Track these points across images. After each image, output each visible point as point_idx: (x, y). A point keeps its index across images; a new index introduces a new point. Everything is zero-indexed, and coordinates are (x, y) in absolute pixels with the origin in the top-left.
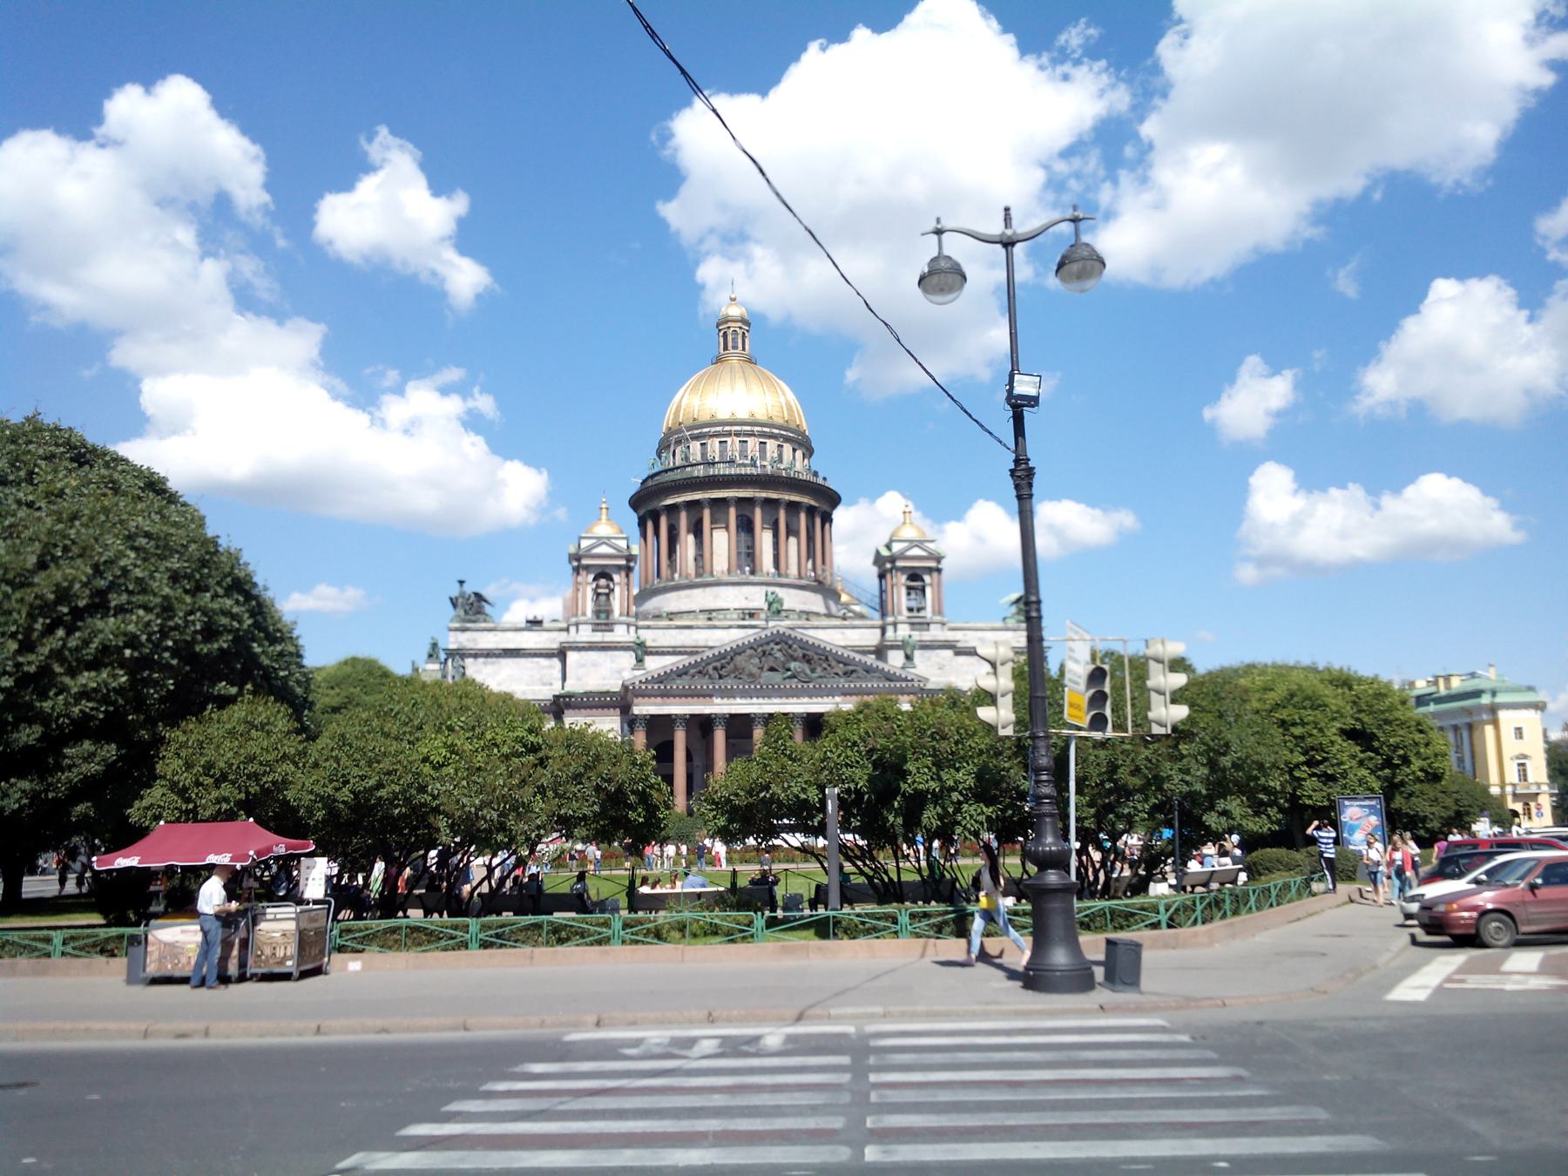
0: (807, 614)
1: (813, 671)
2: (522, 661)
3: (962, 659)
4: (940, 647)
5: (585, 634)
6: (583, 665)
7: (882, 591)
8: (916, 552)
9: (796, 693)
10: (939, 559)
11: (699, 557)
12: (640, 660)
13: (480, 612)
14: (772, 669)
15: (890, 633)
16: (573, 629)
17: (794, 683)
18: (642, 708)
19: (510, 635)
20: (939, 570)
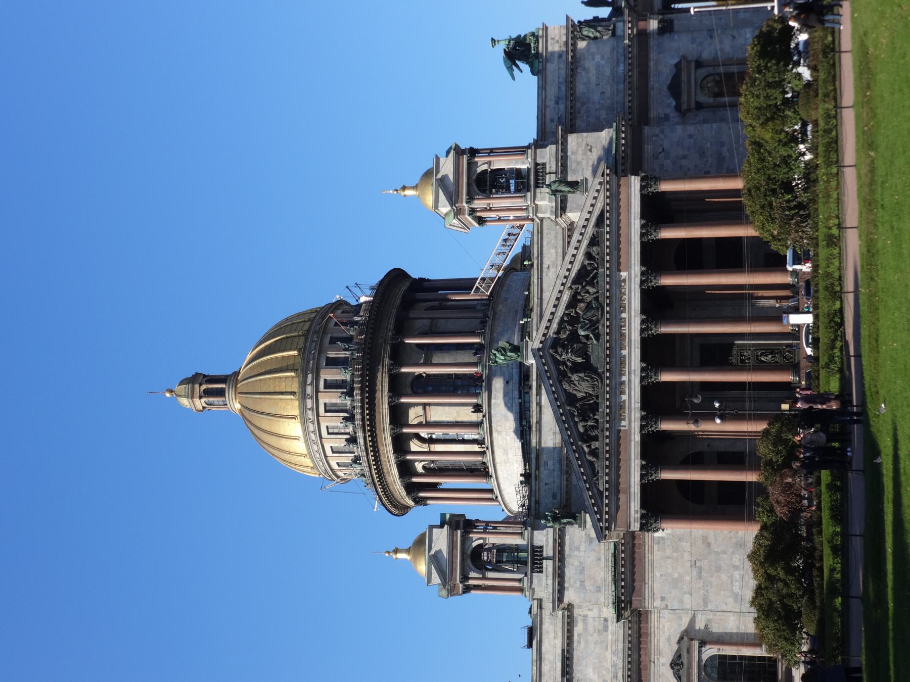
2: (576, 654)
3: (579, 123)
4: (564, 150)
5: (543, 584)
6: (582, 582)
7: (500, 219)
9: (617, 327)
10: (459, 152)
14: (587, 357)
16: (539, 594)
17: (603, 330)
19: (546, 668)
20: (473, 152)
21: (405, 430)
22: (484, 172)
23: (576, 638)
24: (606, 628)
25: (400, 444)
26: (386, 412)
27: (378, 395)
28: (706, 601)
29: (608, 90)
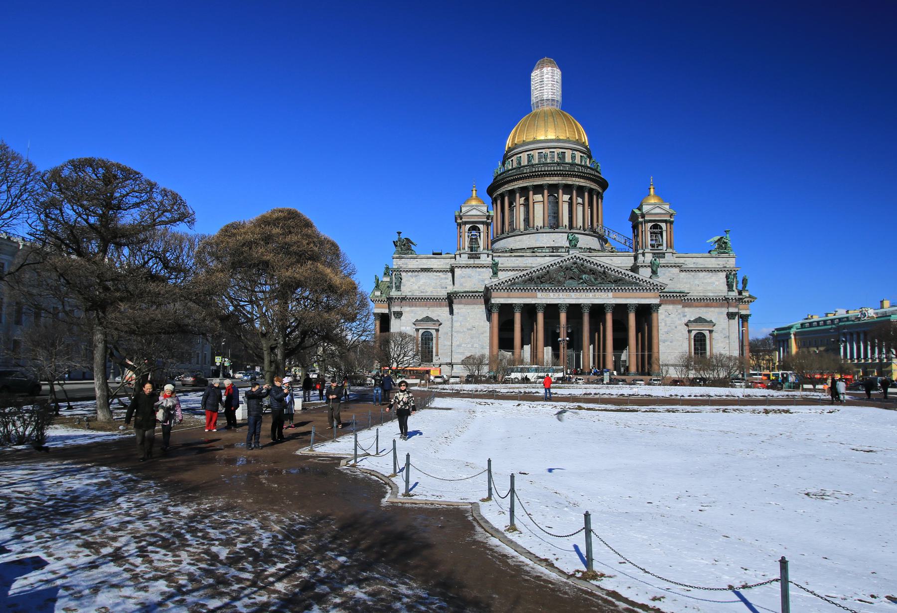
0: (590, 250)
1: (596, 279)
3: (684, 273)
8: (658, 211)
11: (527, 220)
12: (495, 273)
13: (409, 249)
14: (572, 278)
15: (641, 258)
16: (458, 257)
18: (498, 299)
19: (424, 261)
21: (531, 193)
22: (661, 228)
23: (438, 274)
24: (442, 288)
25: (524, 191)
26: (539, 183)
27: (548, 179)
28: (458, 332)
29: (700, 288)
